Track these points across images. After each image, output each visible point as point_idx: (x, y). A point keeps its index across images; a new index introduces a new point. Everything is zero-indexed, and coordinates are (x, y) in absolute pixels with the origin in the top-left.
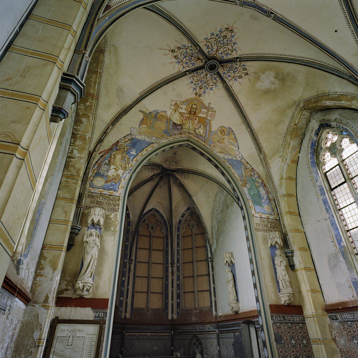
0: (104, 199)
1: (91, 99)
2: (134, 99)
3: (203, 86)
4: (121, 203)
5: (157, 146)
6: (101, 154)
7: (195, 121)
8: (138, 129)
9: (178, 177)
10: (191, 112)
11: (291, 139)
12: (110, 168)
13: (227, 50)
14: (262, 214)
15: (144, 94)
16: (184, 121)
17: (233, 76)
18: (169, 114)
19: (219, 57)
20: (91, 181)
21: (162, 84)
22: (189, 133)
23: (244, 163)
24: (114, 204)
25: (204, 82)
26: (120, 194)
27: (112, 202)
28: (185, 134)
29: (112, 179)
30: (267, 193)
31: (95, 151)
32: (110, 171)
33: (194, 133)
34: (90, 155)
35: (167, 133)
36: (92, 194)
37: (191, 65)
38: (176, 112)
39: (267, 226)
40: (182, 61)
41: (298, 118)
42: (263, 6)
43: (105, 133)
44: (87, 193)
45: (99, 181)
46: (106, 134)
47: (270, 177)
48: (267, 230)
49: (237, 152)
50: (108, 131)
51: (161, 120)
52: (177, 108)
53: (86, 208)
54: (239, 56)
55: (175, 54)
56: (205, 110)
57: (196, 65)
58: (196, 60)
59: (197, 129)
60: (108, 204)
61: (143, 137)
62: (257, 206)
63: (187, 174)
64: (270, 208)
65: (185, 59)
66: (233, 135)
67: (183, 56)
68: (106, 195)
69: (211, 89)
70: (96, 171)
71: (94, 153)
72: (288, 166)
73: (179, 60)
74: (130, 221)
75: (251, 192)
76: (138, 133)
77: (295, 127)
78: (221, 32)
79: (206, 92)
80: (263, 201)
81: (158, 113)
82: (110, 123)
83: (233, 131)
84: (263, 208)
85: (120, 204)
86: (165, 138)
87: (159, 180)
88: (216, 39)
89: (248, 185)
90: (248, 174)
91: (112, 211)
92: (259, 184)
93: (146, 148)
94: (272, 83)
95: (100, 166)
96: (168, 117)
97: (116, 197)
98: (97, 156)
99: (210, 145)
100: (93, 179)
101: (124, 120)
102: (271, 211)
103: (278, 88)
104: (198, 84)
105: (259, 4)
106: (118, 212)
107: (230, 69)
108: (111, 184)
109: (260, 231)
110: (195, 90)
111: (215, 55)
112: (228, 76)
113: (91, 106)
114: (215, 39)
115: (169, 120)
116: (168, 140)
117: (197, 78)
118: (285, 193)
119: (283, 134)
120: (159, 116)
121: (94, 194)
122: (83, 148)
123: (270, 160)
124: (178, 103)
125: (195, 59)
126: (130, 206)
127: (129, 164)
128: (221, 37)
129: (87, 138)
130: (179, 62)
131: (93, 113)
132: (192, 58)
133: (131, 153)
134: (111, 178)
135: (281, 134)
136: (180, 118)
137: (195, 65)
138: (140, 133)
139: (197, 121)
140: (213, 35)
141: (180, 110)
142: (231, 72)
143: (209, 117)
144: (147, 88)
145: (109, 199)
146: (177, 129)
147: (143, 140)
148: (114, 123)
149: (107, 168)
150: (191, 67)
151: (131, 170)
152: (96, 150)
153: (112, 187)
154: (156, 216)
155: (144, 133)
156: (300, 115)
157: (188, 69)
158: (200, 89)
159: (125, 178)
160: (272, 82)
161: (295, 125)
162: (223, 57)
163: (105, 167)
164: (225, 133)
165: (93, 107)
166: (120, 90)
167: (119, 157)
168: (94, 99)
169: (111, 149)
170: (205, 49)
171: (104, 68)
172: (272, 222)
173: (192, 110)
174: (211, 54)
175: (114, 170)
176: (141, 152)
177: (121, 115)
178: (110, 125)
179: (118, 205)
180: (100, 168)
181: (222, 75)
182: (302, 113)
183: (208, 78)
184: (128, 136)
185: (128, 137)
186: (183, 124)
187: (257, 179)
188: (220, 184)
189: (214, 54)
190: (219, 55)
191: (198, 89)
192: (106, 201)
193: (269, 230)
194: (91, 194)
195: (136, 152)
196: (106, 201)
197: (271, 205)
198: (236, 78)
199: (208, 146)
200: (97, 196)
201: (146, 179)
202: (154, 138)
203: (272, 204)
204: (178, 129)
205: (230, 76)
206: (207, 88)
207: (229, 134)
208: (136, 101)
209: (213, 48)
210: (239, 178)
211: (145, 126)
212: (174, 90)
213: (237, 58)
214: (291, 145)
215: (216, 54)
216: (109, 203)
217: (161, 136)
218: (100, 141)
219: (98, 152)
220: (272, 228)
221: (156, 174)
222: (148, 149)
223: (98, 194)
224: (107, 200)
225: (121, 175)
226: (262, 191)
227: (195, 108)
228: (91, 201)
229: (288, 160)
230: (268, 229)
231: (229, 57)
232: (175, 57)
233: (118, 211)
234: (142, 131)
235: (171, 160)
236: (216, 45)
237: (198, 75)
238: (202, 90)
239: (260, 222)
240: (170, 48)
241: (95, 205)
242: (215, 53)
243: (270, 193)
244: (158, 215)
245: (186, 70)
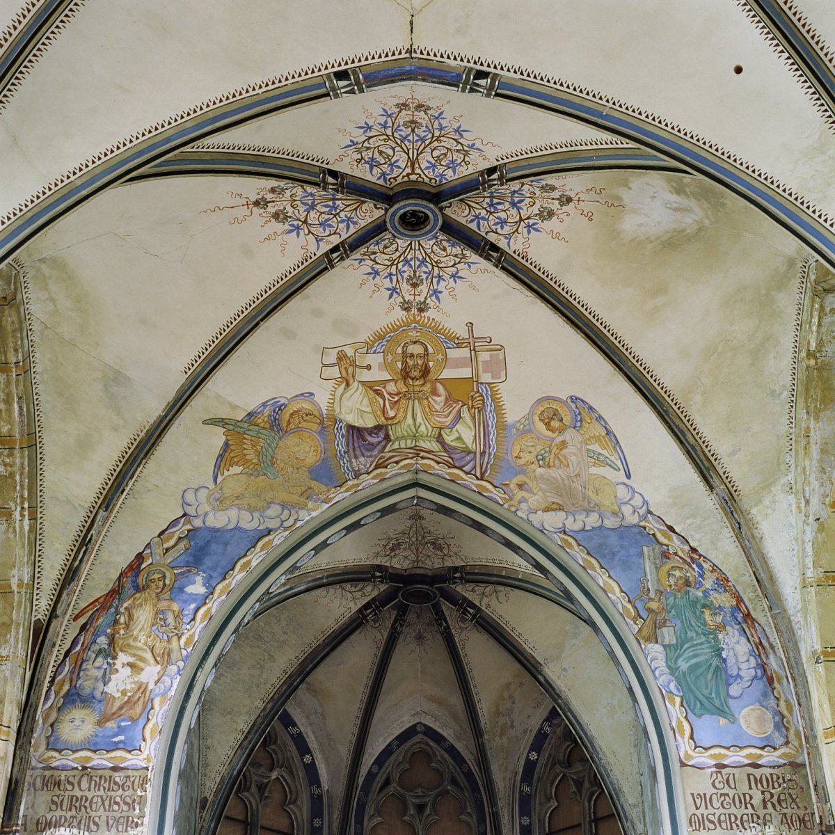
0: (95, 786)
1: (6, 452)
2: (171, 395)
3: (422, 274)
4: (151, 793)
5: (286, 538)
6: (82, 620)
7: (435, 398)
8: (212, 486)
9: (468, 595)
10: (407, 373)
11: (808, 413)
12: (114, 664)
14: (728, 748)
15: (199, 370)
16: (392, 409)
17: (517, 219)
18: (322, 400)
19: (431, 179)
20: (52, 726)
21: (256, 316)
22: (417, 452)
23: (654, 535)
24: (128, 800)
25: (417, 263)
26: (148, 759)
27: (120, 792)
28: (397, 462)
29: (121, 708)
30: (760, 649)
31: (56, 617)
32: (113, 677)
33: (435, 446)
34: (40, 635)
35: (325, 474)
36: (56, 773)
37: (341, 226)
38: (348, 385)
39: (745, 801)
40: (305, 222)
41: (814, 328)
42: (445, 60)
43: (84, 543)
44: (38, 772)
45: (77, 722)
46: (86, 545)
47: (765, 582)
48: (745, 818)
49: (622, 492)
50: (93, 532)
51: (298, 429)
52: (350, 369)
53: (37, 827)
54: (496, 164)
55: (272, 209)
56: (464, 353)
57: (360, 221)
58: (354, 206)
59: (447, 427)
60: (107, 803)
61: (233, 513)
62: (706, 717)
63: (490, 588)
64: (769, 715)
65: (312, 214)
66: (597, 425)
67: (302, 208)
68: (100, 772)
69: (453, 276)
70: (66, 687)
71: (54, 623)
72: (821, 529)
73: (295, 223)
74: (320, 797)
75: (680, 660)
76: (213, 503)
77: (812, 362)
80: (734, 690)
81: (281, 407)
82: (99, 502)
83: (591, 408)
84: (732, 718)
85: (149, 796)
86: (319, 499)
87: (395, 621)
89: (668, 634)
90: (672, 581)
91: (120, 828)
92: (719, 619)
93: (245, 555)
94: (676, 210)
95: (79, 663)
96: (325, 412)
97: (135, 773)
98: (64, 632)
99: (504, 487)
100: (57, 719)
101: (151, 471)
102: (770, 728)
103: (707, 222)
104: (399, 271)
105: (432, 57)
106: (139, 829)
107: (495, 201)
108: (119, 727)
109: (712, 826)
110: (397, 293)
111: (413, 177)
112: (496, 224)
113: (12, 475)
115: (327, 423)
116: (328, 506)
117: (388, 257)
118: (818, 647)
119: (785, 393)
120: (286, 416)
121: (60, 772)
122: (4, 624)
123: (756, 505)
124: (349, 352)
125: (348, 206)
126: (313, 732)
127: (180, 638)
128: (399, 126)
129: (14, 587)
130: (298, 228)
131: (22, 496)
132: (338, 202)
133: (190, 589)
134: (117, 704)
135: (780, 394)
136: (371, 403)
137: (355, 223)
138: (221, 503)
139: (442, 398)
141: (366, 376)
142: (499, 207)
143: (485, 371)
144: (276, 279)
145: (112, 784)
146: (368, 450)
147: (231, 530)
148: (111, 500)
149: (105, 666)
150: (343, 233)
151: (185, 660)
152: (59, 612)
153: (122, 738)
154: (435, 755)
155: (237, 498)
156: (816, 314)
157: (335, 240)
158: (414, 285)
159: (164, 694)
160: (675, 205)
161: (810, 355)
162: (442, 175)
163: (97, 664)
164: (561, 420)
165: (18, 478)
166: (115, 379)
167: (144, 616)
168: (17, 453)
169: (115, 593)
170: (363, 173)
171: (35, 337)
172: (770, 781)
173: (411, 362)
174: (395, 179)
175: (128, 670)
176: (224, 578)
177: (132, 464)
178: (98, 510)
179: (142, 801)
180: (79, 674)
181: (473, 226)
182: (822, 308)
183: (428, 247)
184: (175, 526)
185: (174, 529)
186: (390, 422)
187: (714, 595)
188: (517, 654)
189: (408, 175)
190: (426, 172)
191: (405, 287)
192: (102, 793)
193: (754, 818)
194: (52, 776)
195: (204, 585)
196: (102, 793)
197: (772, 702)
198: (531, 222)
199: (497, 494)
200: (71, 779)
201: (340, 627)
202: (274, 510)
203: (778, 699)
204: (372, 446)
205: (503, 222)
206: (440, 277)
207: (581, 421)
208: (176, 401)
209: (393, 161)
210: (629, 606)
211: (237, 469)
212: (317, 313)
213: (491, 171)
214: (815, 436)
215: (413, 173)
216: (111, 797)
217: (302, 495)
218: (70, 575)
219: (64, 618)
220: (769, 805)
221: (374, 600)
222: (249, 563)
223: (76, 772)
224: (104, 788)
225: (151, 686)
226: (736, 647)
227: (419, 355)
228: (52, 800)
229: (815, 501)
230: (750, 811)
231: (464, 172)
232: (276, 216)
233: (142, 824)
234: (227, 492)
235: (414, 539)
237: (386, 247)
238: (424, 288)
239: (715, 788)
240: (245, 200)
241: (64, 813)
242: (408, 170)
243: (772, 647)
244: (440, 752)
245: (331, 246)
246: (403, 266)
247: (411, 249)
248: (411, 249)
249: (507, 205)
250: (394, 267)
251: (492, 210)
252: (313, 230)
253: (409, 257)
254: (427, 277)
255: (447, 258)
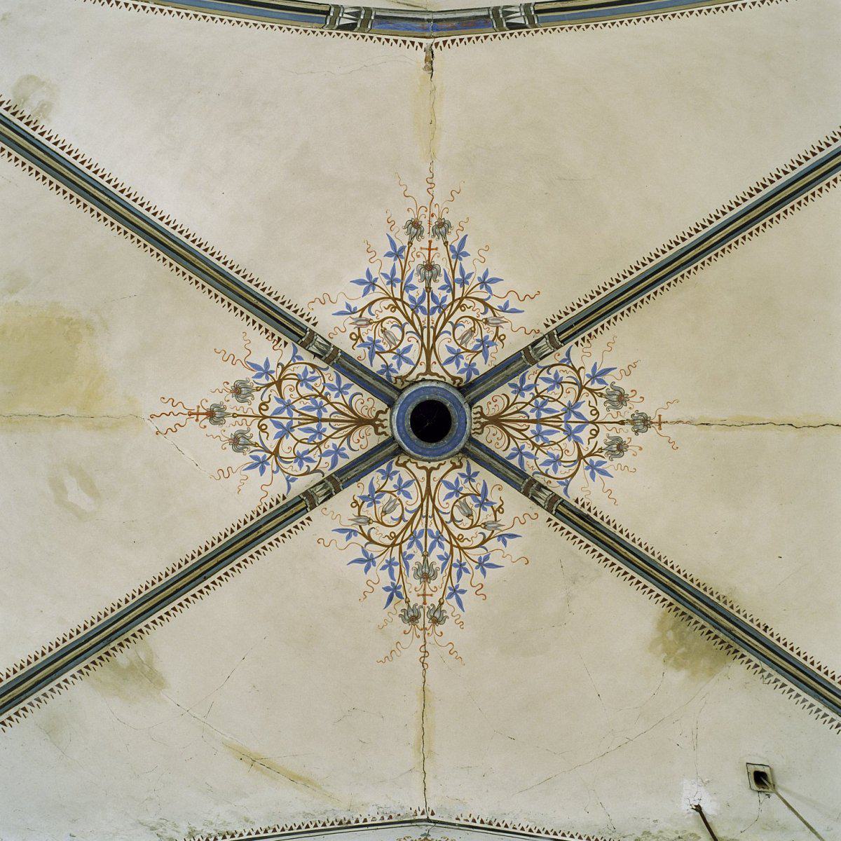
13: (385, 512)
67: (584, 410)
69: (372, 284)
73: (596, 386)
78: (455, 591)
79: (389, 255)
88: (458, 546)
114: (461, 544)
125: (518, 412)
130: (593, 378)
140: (483, 564)
158: (429, 266)
174: (455, 467)
236: (447, 518)
238: (416, 262)
246: (444, 299)
247: (435, 329)
248: (435, 329)
249: (298, 406)
250: (458, 294)
251: (318, 400)
252: (574, 374)
253: (437, 314)
254: (410, 278)
255: (381, 318)
